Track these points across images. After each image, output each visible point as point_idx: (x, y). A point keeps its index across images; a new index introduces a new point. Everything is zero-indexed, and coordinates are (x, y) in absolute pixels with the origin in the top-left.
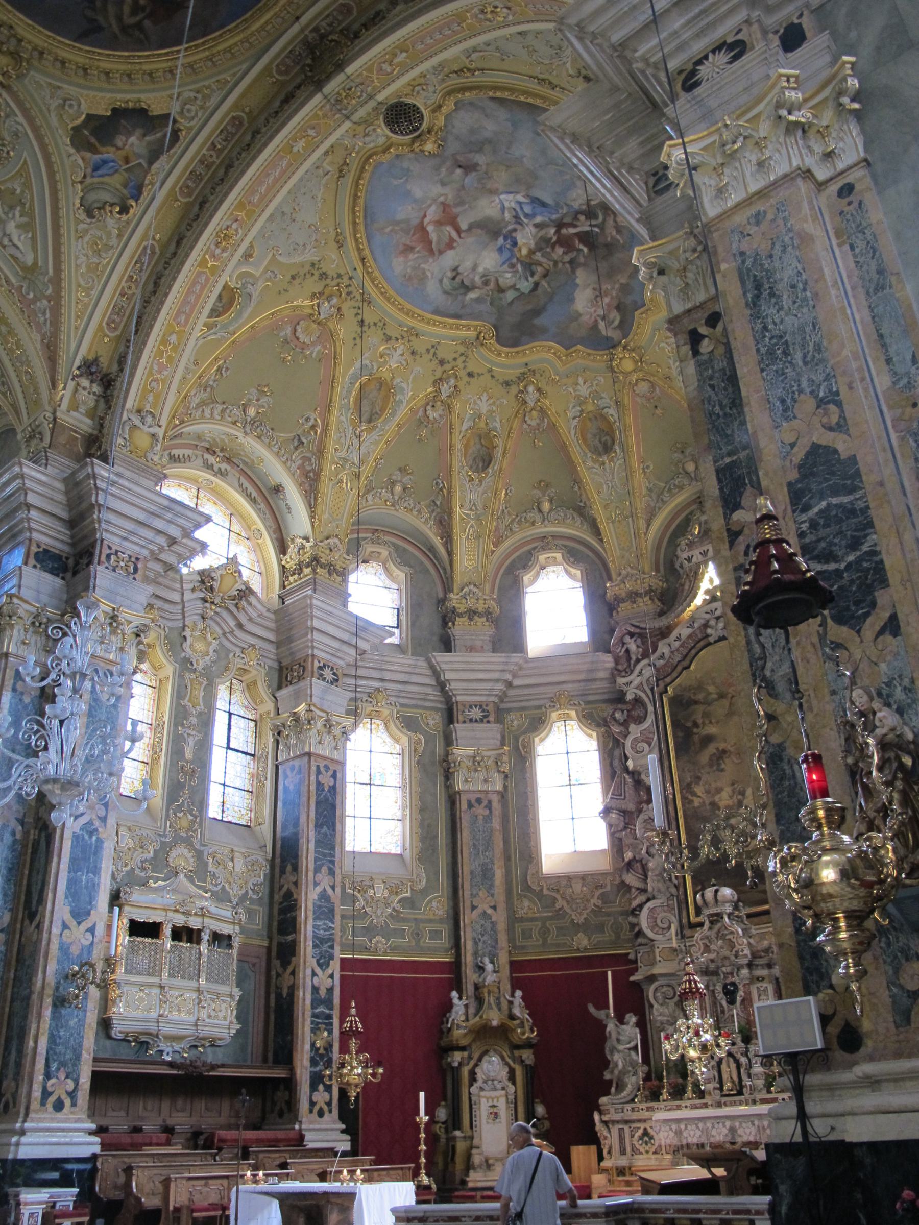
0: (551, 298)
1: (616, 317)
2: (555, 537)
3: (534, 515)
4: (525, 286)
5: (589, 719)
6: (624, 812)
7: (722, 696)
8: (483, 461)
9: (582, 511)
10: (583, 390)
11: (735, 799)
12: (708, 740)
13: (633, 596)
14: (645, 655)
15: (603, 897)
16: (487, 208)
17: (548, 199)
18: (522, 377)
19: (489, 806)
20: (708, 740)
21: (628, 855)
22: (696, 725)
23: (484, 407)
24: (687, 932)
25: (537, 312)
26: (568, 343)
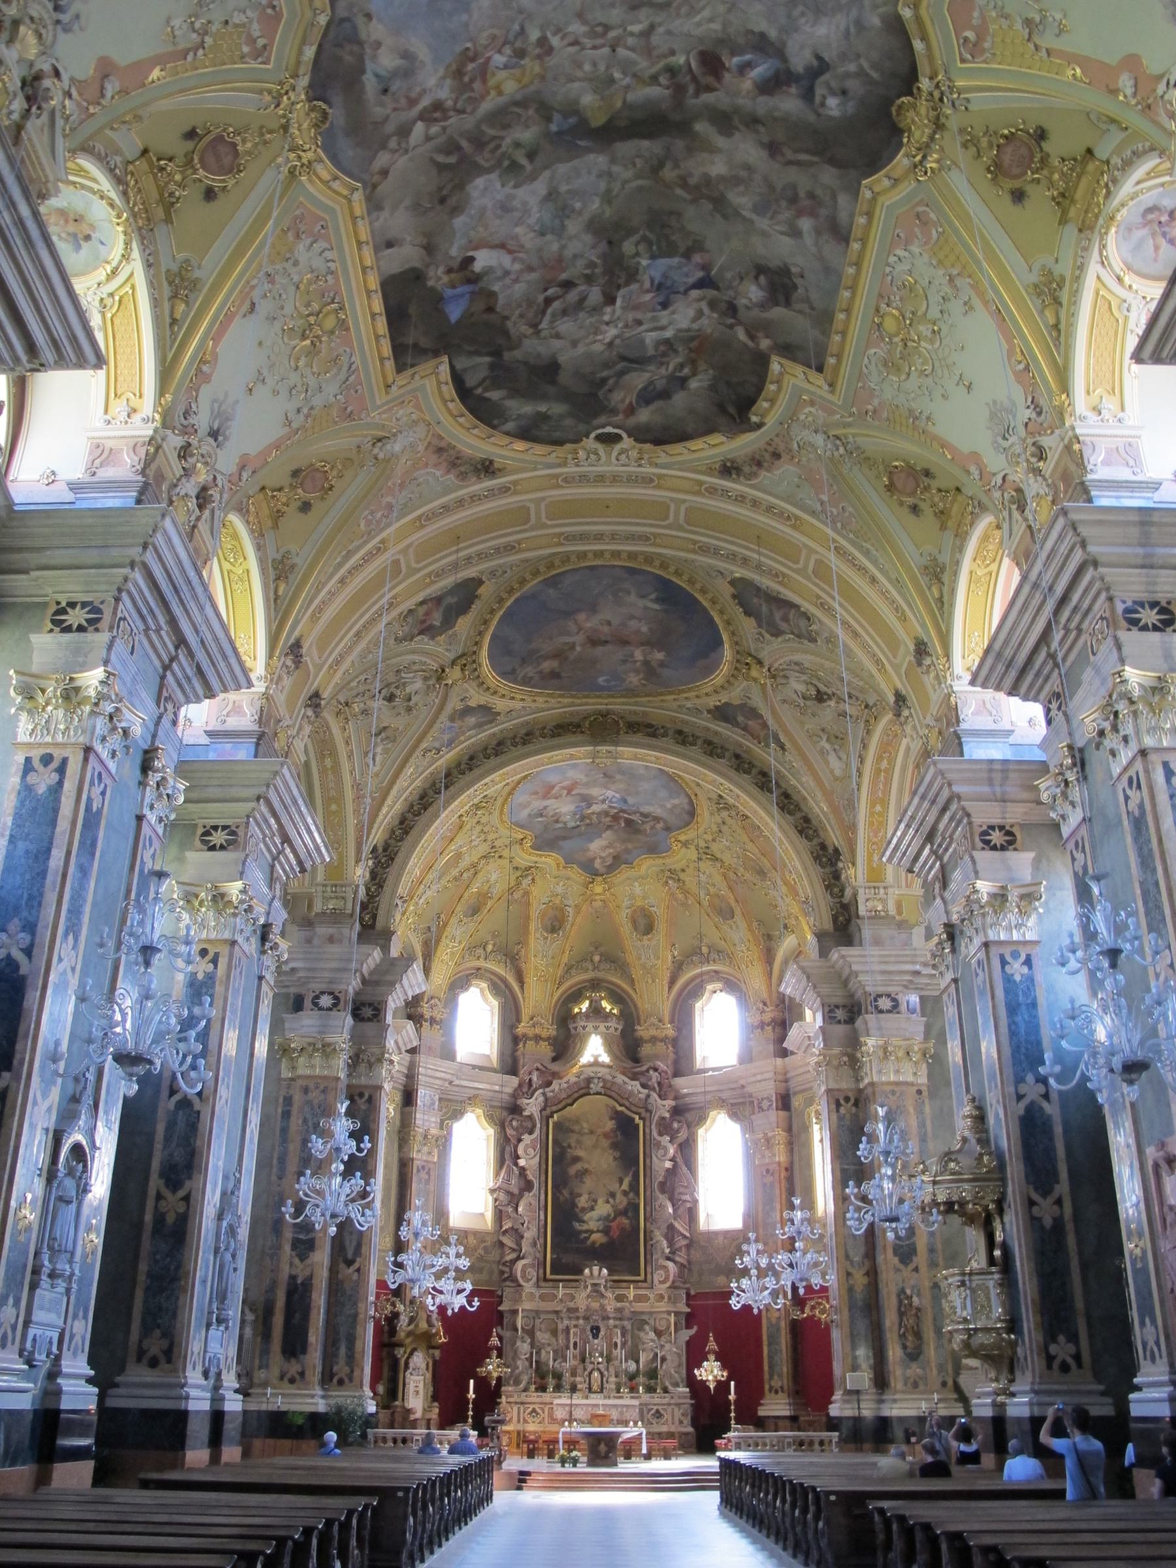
0: (580, 835)
1: (609, 861)
2: (487, 970)
3: (480, 951)
4: (571, 824)
5: (490, 1118)
6: (509, 1193)
7: (591, 1132)
8: (475, 911)
9: (513, 959)
10: (559, 889)
11: (590, 1203)
12: (577, 1159)
13: (538, 1038)
14: (541, 1087)
15: (485, 1248)
16: (595, 792)
17: (631, 800)
18: (529, 868)
19: (428, 1173)
20: (577, 1159)
21: (507, 1225)
22: (570, 1146)
23: (494, 877)
24: (542, 1284)
25: (564, 838)
26: (569, 861)
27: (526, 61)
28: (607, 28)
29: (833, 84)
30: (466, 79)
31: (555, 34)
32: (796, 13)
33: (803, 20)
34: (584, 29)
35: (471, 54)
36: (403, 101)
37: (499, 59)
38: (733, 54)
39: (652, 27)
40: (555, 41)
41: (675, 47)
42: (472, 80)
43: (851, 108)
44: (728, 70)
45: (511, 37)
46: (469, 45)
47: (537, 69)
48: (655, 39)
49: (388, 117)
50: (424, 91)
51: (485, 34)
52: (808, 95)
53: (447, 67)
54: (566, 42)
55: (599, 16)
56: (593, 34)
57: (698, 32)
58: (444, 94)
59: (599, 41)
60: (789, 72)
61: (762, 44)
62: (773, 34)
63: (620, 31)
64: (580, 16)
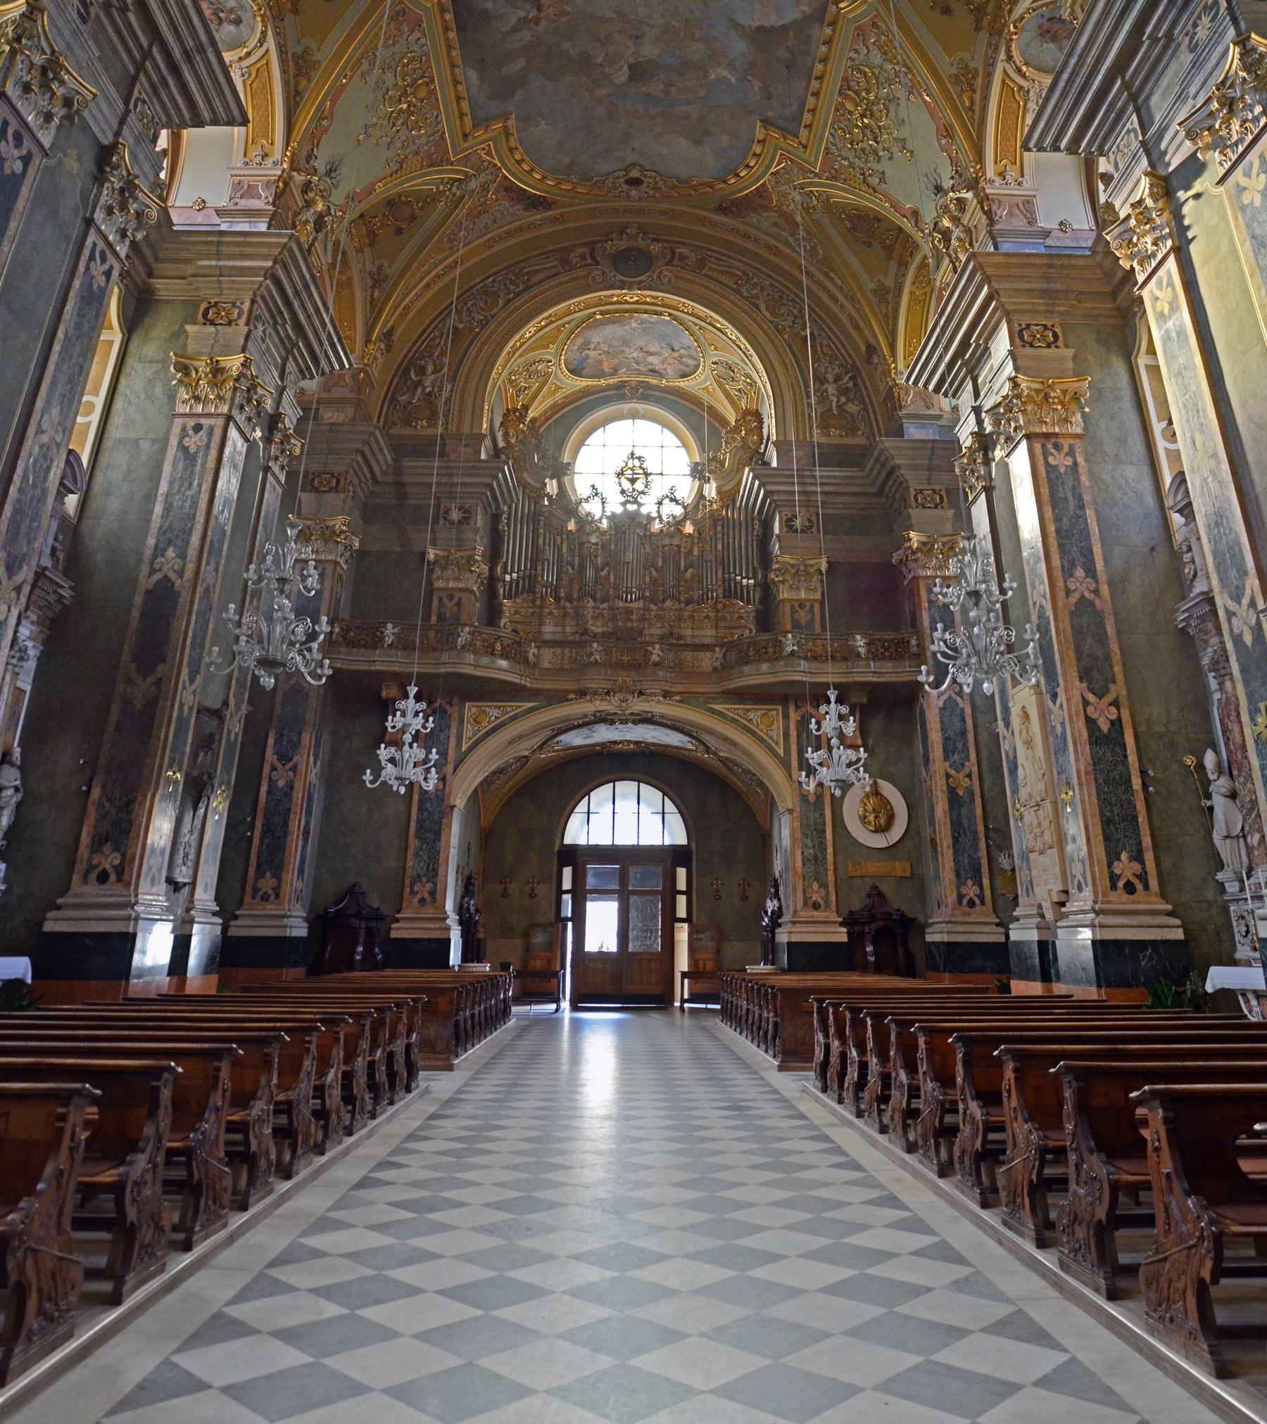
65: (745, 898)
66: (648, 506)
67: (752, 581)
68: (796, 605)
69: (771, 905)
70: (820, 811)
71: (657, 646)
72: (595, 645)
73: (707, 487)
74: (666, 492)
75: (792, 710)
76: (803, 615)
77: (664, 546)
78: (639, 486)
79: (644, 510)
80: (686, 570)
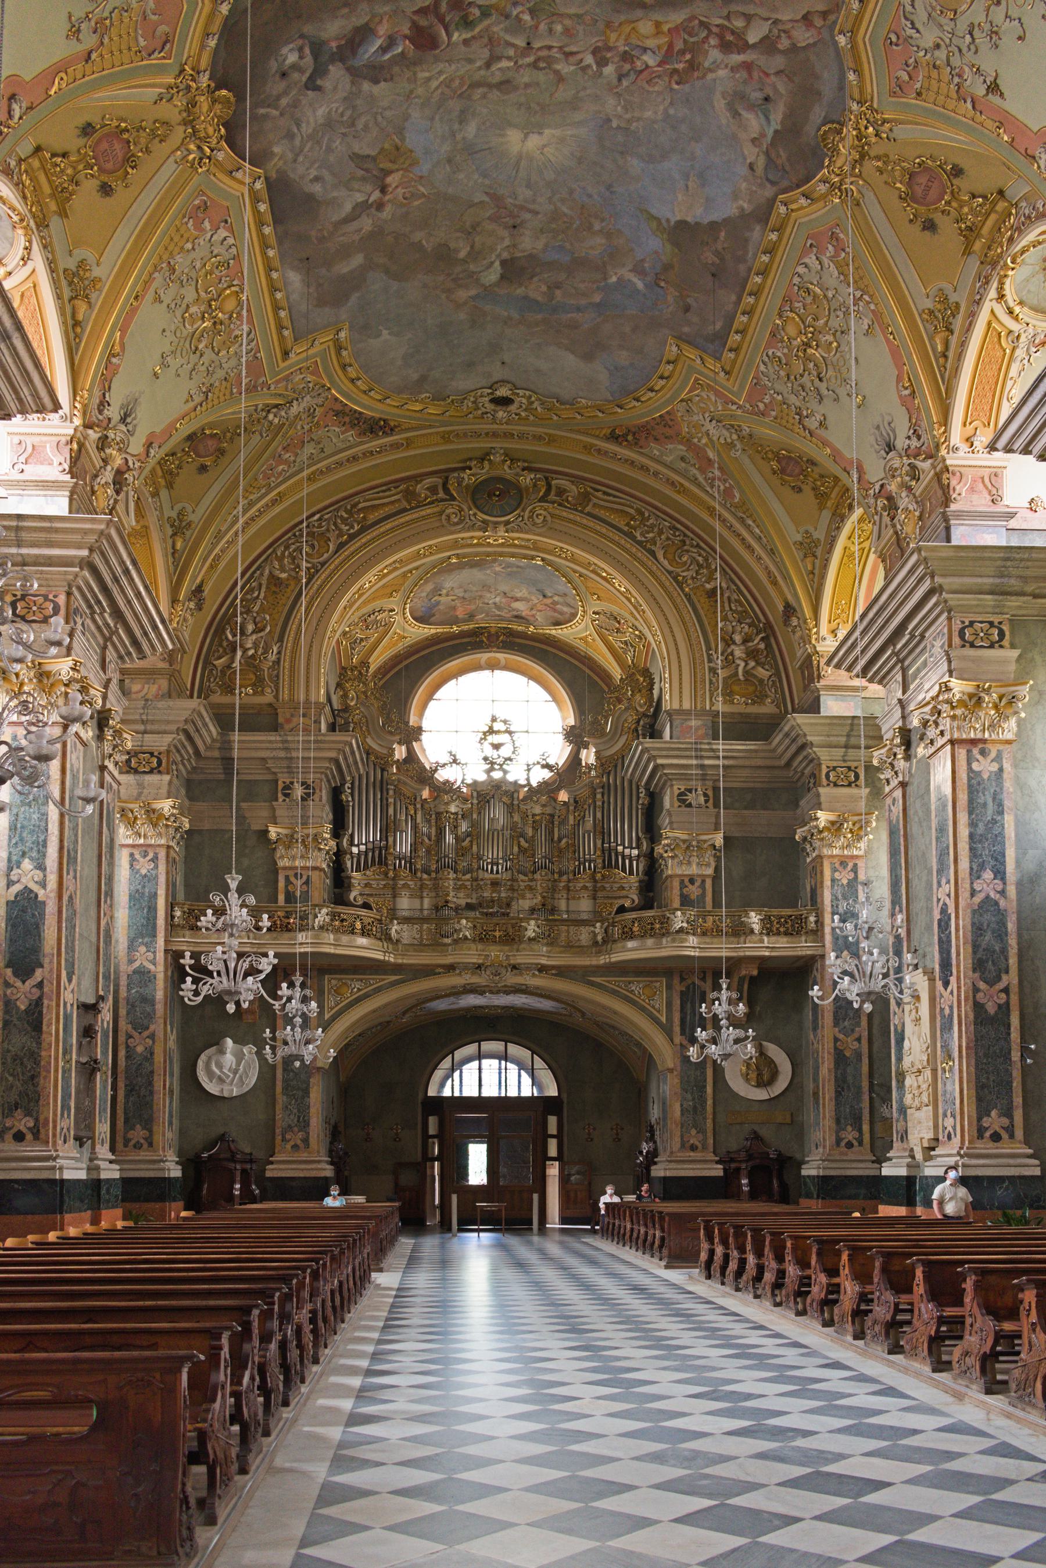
27: (622, 49)
28: (534, 65)
29: (296, 76)
30: (688, 57)
31: (589, 66)
32: (349, 113)
33: (341, 110)
34: (558, 67)
35: (676, 77)
36: (755, 75)
37: (650, 59)
38: (403, 53)
39: (488, 65)
40: (589, 59)
41: (463, 48)
42: (682, 52)
43: (273, 65)
44: (406, 37)
45: (633, 76)
46: (676, 87)
47: (613, 36)
48: (486, 53)
49: (778, 73)
50: (732, 69)
51: (656, 88)
52: (317, 48)
53: (704, 76)
54: (579, 57)
55: (541, 77)
56: (550, 61)
57: (441, 66)
58: (715, 55)
59: (544, 53)
60: (342, 60)
61: (376, 73)
62: (366, 86)
63: (520, 62)
64: (560, 78)
65: (617, 1140)
66: (516, 774)
67: (635, 852)
68: (686, 880)
69: (645, 1148)
70: (701, 1077)
71: (533, 922)
72: (464, 921)
73: (584, 753)
74: (537, 758)
75: (676, 981)
76: (694, 891)
77: (534, 815)
78: (506, 751)
79: (510, 778)
80: (560, 840)
